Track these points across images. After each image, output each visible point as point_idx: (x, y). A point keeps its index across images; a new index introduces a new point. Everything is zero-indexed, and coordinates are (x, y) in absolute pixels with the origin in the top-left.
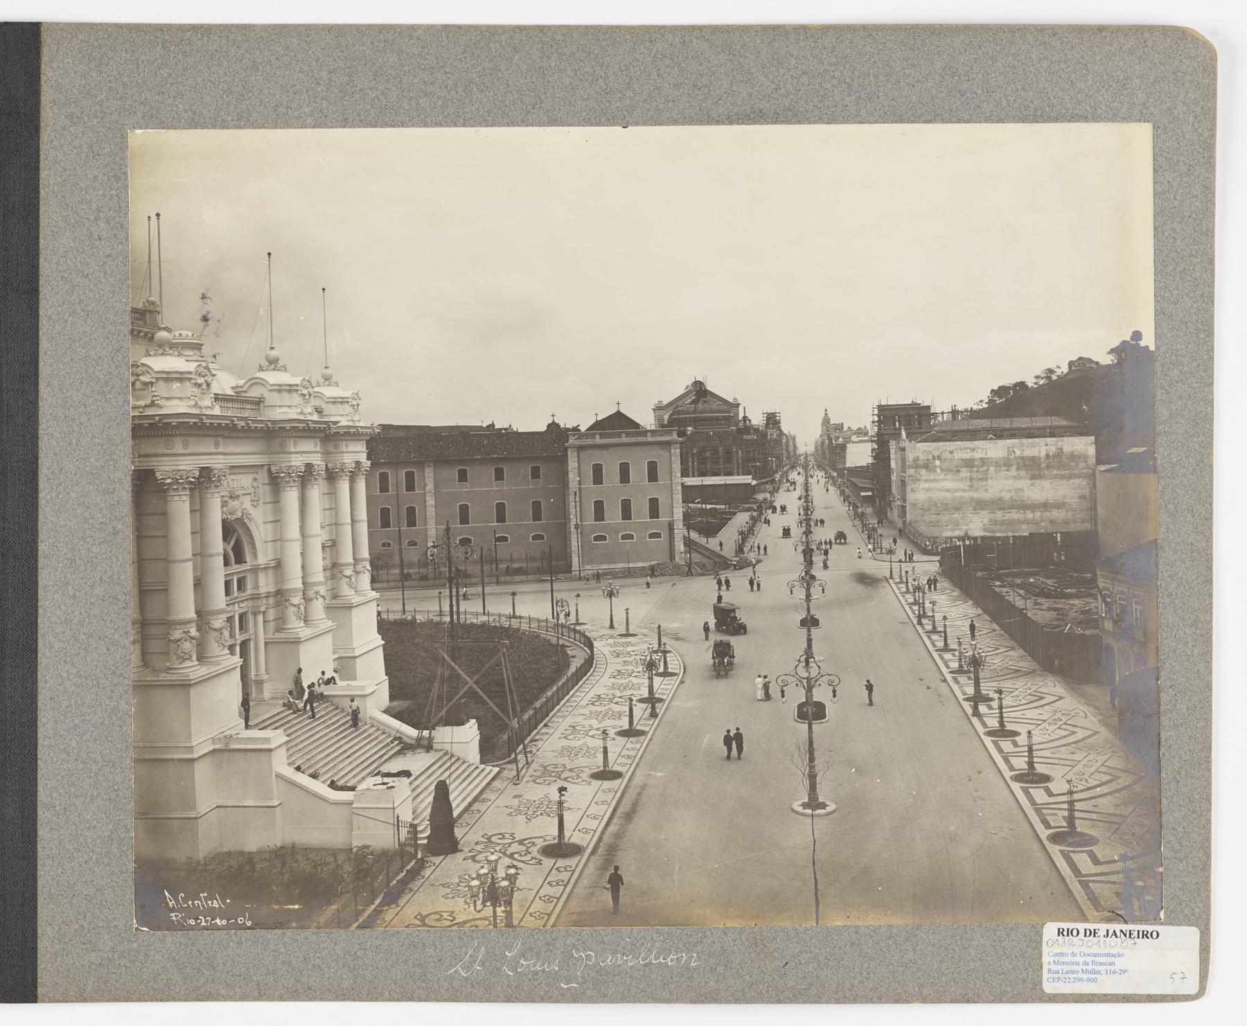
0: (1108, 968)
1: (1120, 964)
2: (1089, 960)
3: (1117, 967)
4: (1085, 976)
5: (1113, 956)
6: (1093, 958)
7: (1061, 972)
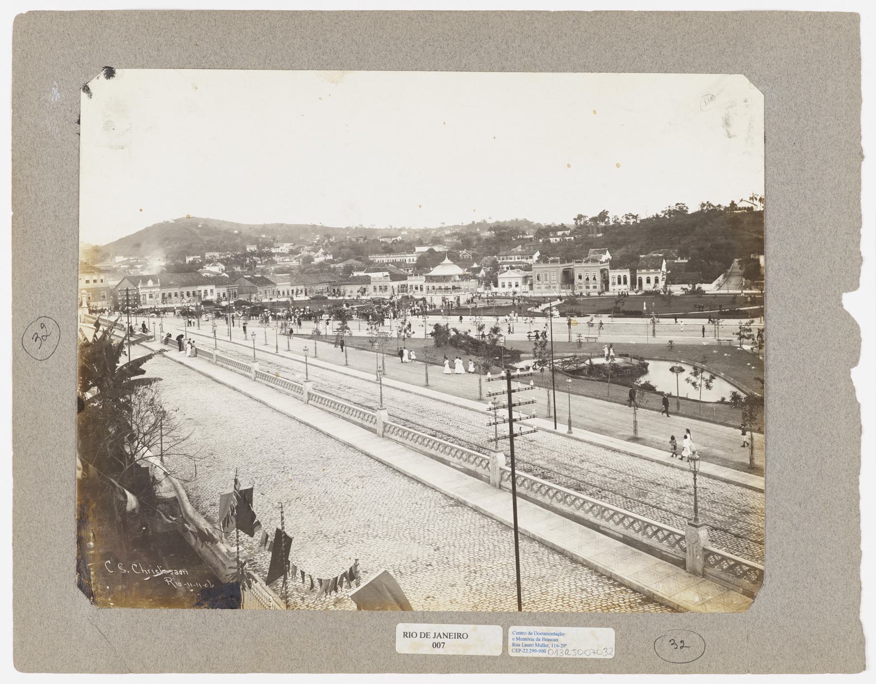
0: (554, 642)
2: (540, 637)
4: (538, 648)
6: (544, 636)
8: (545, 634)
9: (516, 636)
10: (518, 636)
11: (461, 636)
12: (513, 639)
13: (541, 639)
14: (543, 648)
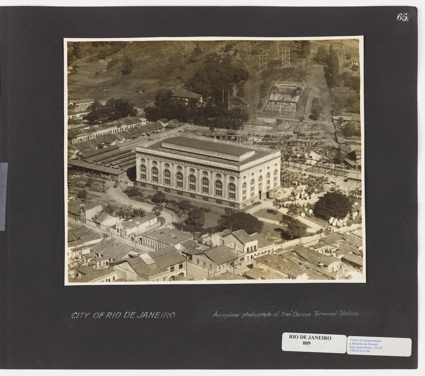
0: (375, 346)
2: (367, 343)
3: (378, 347)
4: (365, 349)
5: (377, 341)
7: (355, 347)
8: (370, 341)
10: (353, 342)
12: (350, 344)
13: (367, 344)
14: (369, 349)
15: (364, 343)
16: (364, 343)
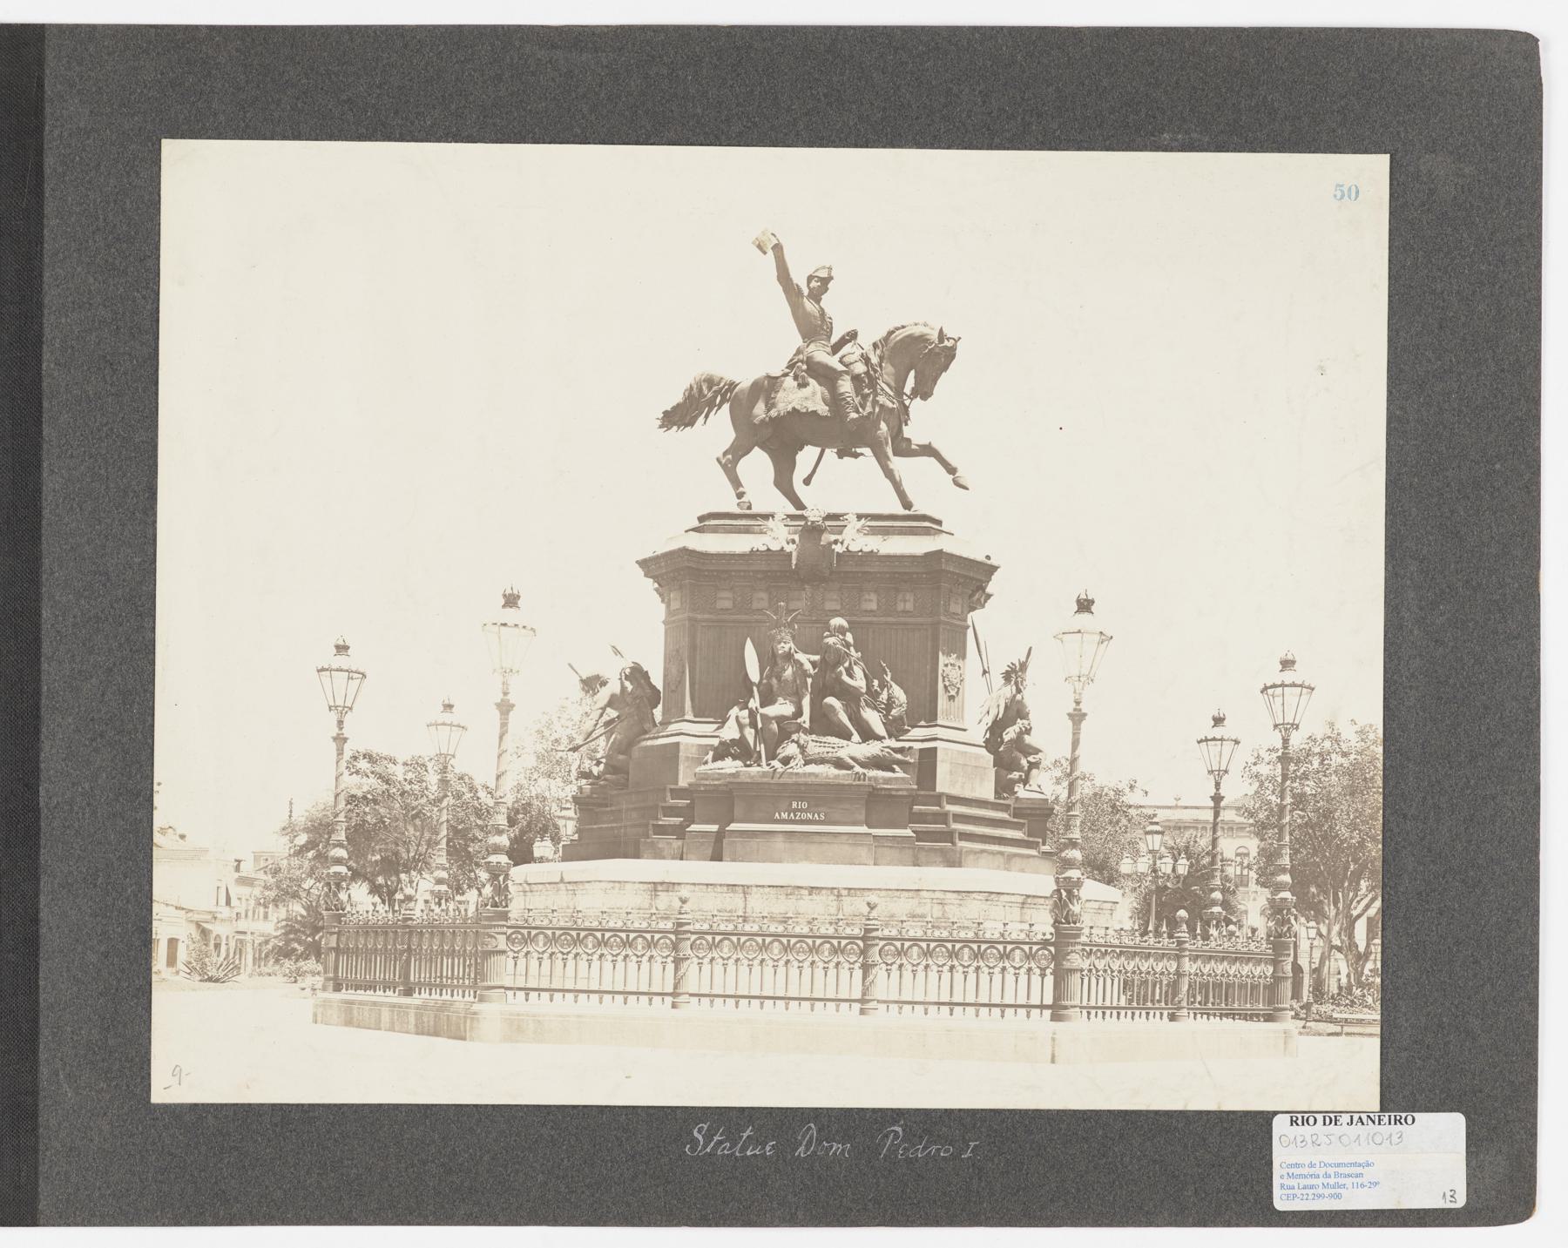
0: (1355, 1180)
1: (1369, 1174)
2: (1331, 1171)
3: (1364, 1180)
4: (1327, 1192)
5: (1360, 1165)
7: (1296, 1187)
9: (1287, 1170)
10: (1291, 1171)
11: (1403, 1121)
12: (1282, 1177)
13: (1333, 1176)
14: (1339, 1191)
15: (1321, 1172)
16: (1322, 1171)
